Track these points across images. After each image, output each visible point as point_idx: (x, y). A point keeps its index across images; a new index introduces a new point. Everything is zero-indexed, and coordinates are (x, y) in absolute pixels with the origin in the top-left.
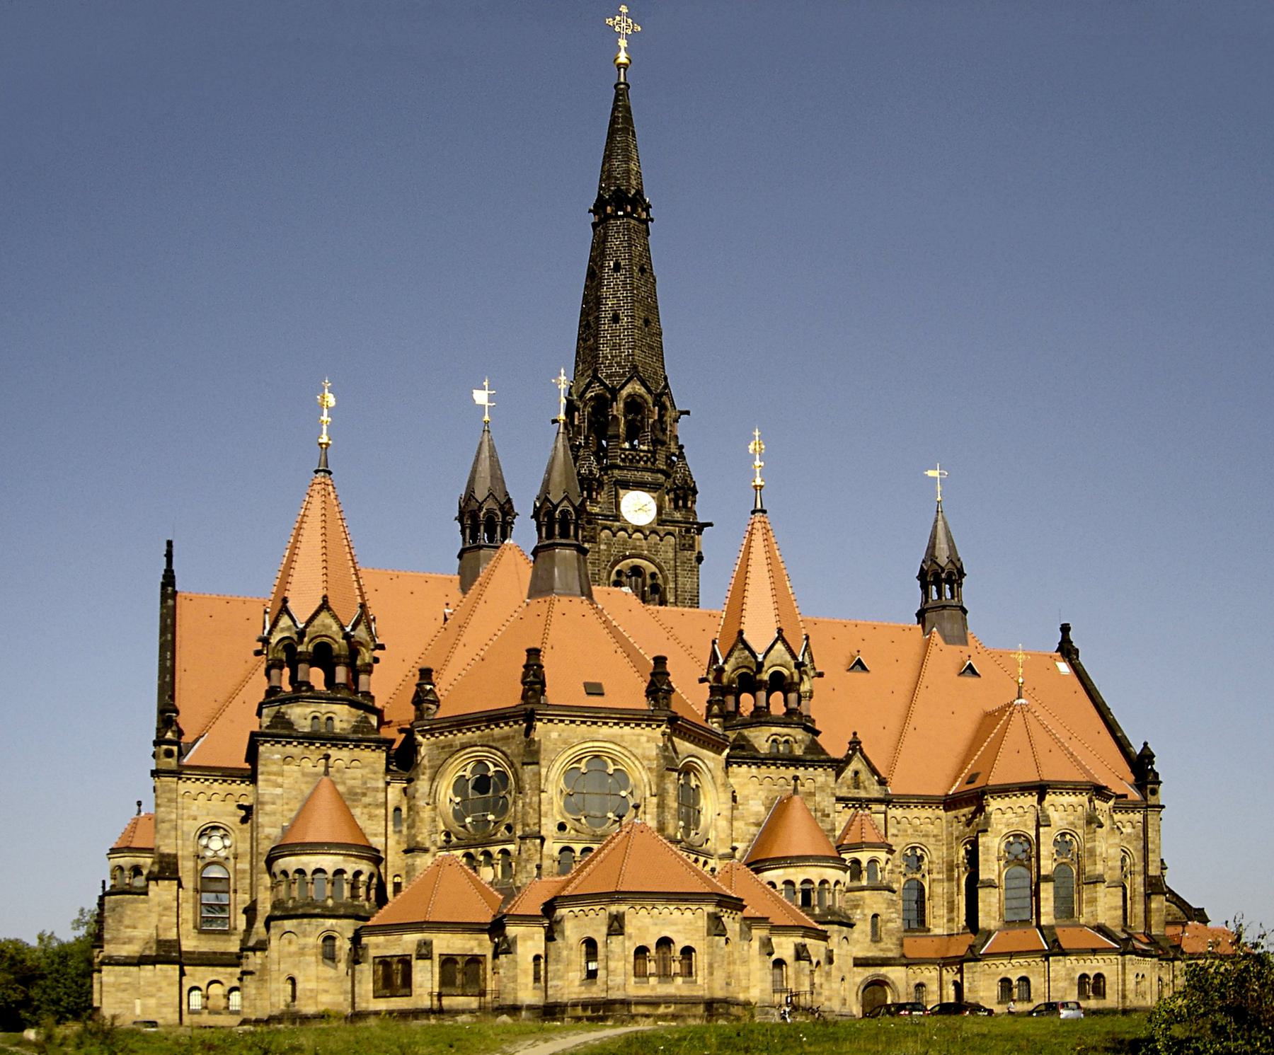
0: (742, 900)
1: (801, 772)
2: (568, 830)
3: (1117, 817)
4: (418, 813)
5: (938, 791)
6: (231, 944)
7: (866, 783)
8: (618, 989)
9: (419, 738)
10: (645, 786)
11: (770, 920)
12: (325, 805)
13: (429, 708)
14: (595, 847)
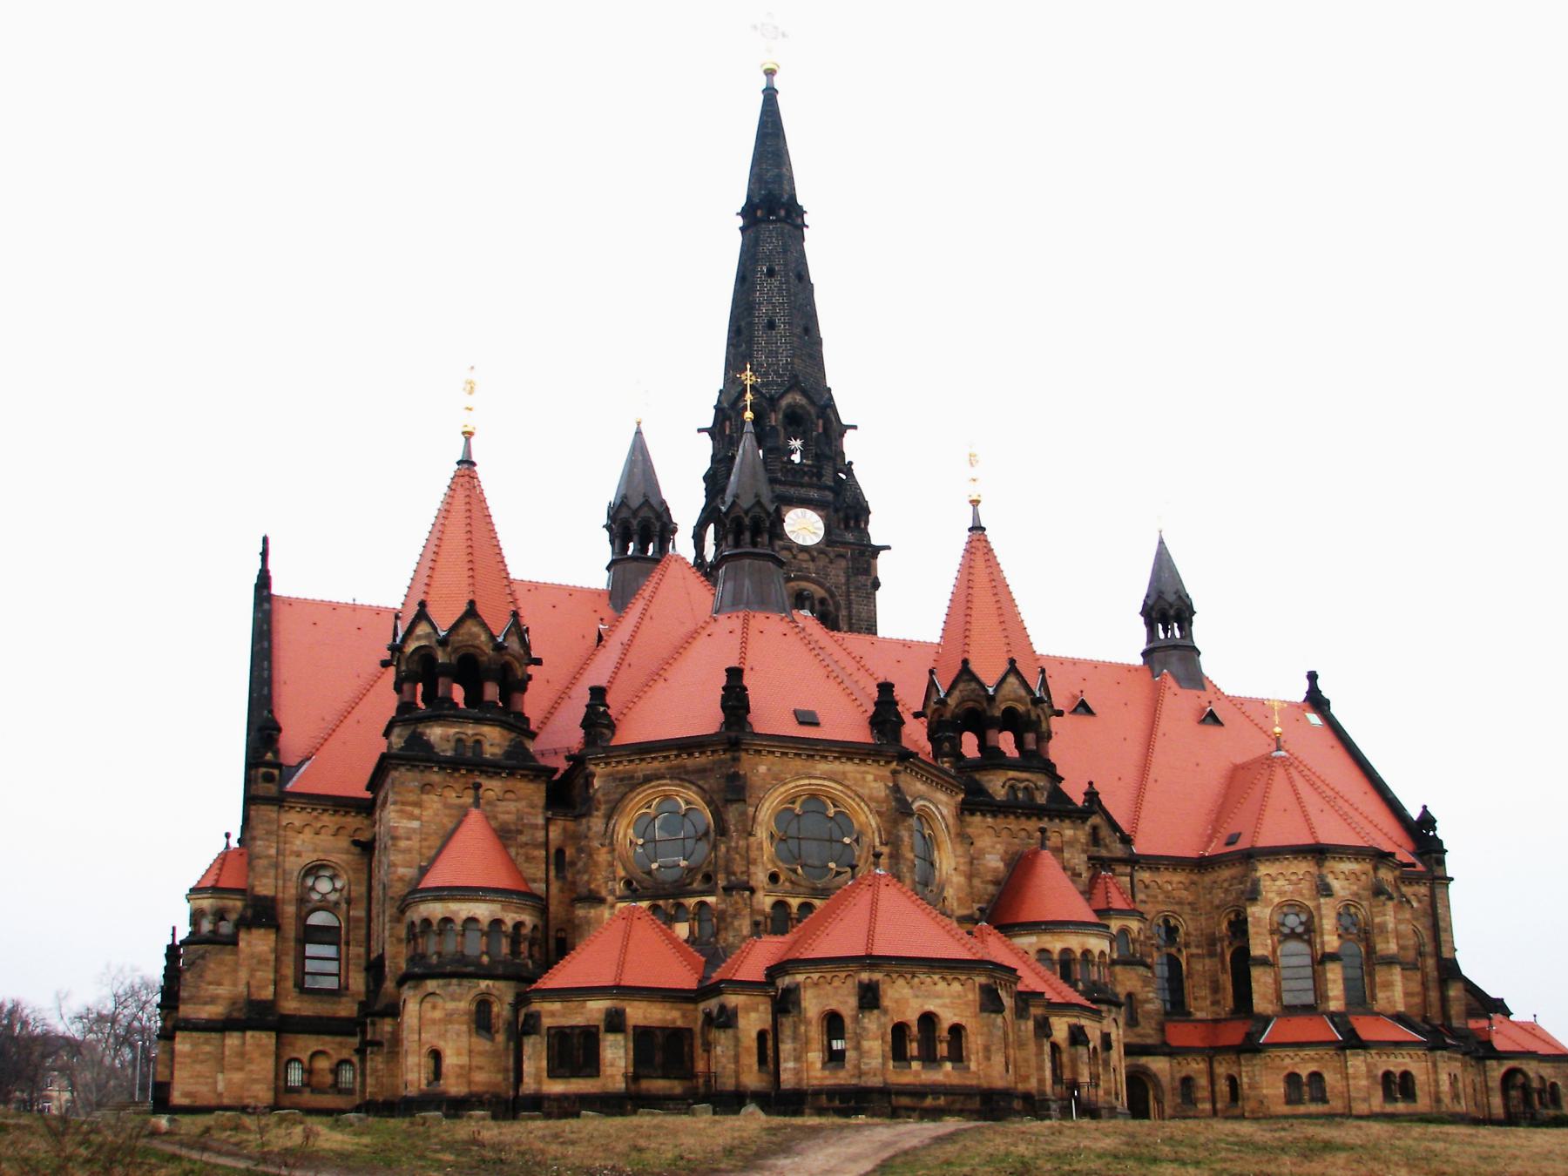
0: (1015, 970)
1: (1044, 824)
4: (590, 855)
7: (1107, 841)
8: (875, 1075)
10: (873, 832)
14: (817, 902)
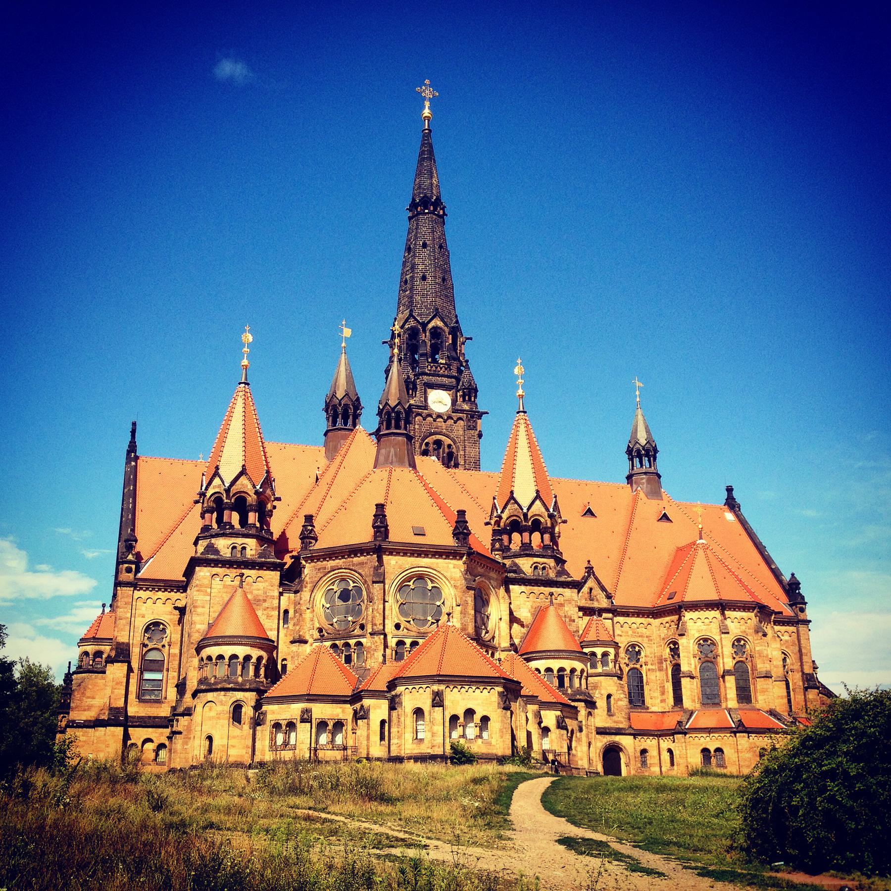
0: (521, 683)
1: (553, 590)
2: (401, 629)
3: (777, 628)
5: (647, 602)
6: (162, 710)
9: (304, 562)
11: (539, 698)
12: (237, 609)
13: (311, 543)
